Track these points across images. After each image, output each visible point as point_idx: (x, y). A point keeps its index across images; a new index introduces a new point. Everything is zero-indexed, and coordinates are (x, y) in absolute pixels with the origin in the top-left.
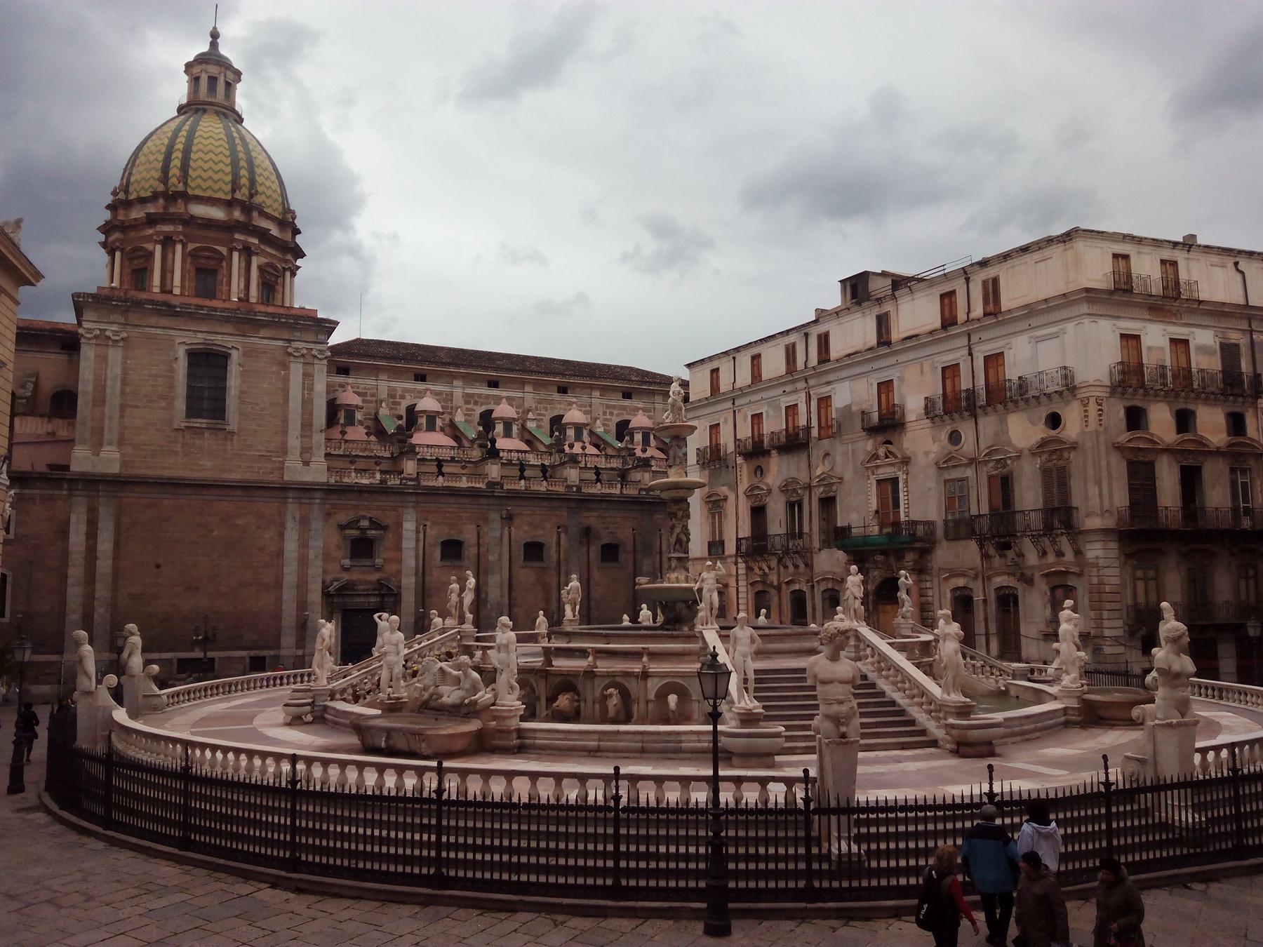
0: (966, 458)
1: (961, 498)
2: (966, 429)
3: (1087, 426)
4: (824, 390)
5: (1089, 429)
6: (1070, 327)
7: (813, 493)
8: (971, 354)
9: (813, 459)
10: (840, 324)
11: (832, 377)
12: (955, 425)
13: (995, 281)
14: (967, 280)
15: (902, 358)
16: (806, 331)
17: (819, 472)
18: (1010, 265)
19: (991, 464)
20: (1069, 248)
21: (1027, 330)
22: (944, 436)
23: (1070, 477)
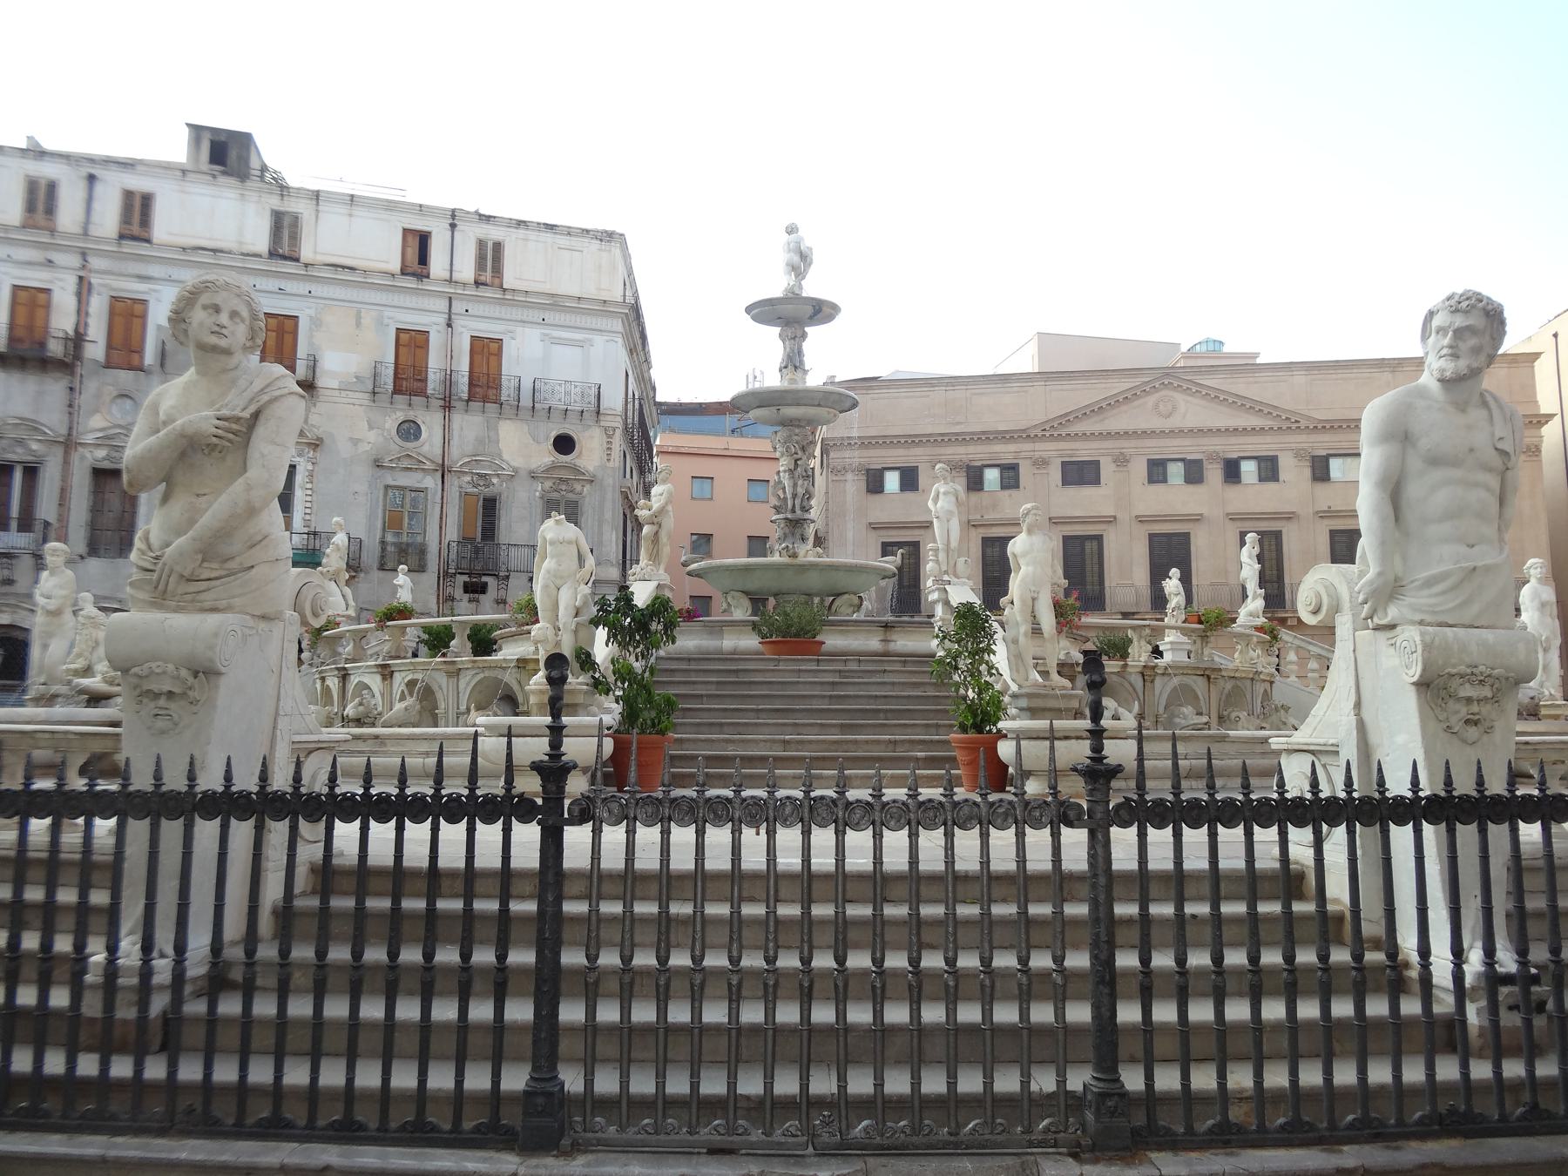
0: (433, 462)
1: (412, 515)
2: (430, 423)
3: (608, 460)
4: (133, 288)
5: (611, 464)
6: (599, 339)
7: (75, 458)
8: (449, 325)
9: (85, 399)
10: (183, 192)
11: (154, 270)
12: (411, 413)
13: (498, 247)
14: (453, 226)
15: (318, 290)
16: (93, 171)
17: (97, 422)
18: (521, 236)
19: (468, 478)
20: (605, 250)
21: (539, 324)
22: (391, 422)
23: (582, 515)
